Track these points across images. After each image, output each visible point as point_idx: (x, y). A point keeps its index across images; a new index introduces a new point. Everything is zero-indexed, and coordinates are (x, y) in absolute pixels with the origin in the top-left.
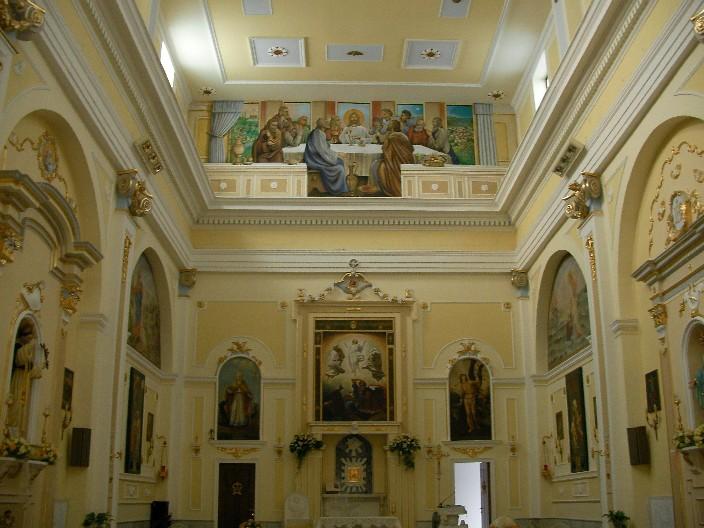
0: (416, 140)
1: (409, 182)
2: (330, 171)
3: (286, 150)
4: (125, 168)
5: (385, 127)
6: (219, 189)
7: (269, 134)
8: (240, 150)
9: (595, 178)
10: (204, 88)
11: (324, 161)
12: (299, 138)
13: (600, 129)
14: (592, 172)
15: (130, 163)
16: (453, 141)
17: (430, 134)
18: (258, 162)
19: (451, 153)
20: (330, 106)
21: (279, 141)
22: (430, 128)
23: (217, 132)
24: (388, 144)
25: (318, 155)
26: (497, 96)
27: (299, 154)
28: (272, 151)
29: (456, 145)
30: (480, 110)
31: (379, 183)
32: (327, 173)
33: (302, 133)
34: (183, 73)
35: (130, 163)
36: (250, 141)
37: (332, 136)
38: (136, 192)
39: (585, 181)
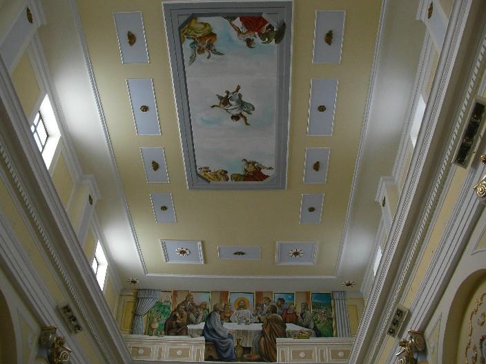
0: (288, 320)
1: (283, 352)
2: (222, 343)
3: (189, 327)
4: (48, 325)
5: (265, 310)
6: (138, 355)
7: (178, 315)
8: (156, 325)
9: (420, 334)
10: (131, 279)
11: (219, 336)
12: (200, 317)
13: (421, 296)
14: (416, 330)
15: (53, 320)
16: (316, 320)
17: (299, 315)
18: (168, 335)
19: (315, 328)
20: (224, 294)
21: (185, 319)
22: (299, 310)
23: (140, 312)
24: (268, 323)
25: (214, 331)
26: (349, 285)
27: (199, 330)
28: (179, 327)
29: (319, 322)
30: (336, 296)
31: (260, 352)
32: (220, 344)
33: (202, 314)
34: (115, 269)
35: (53, 320)
36: (164, 319)
37: (225, 317)
38: (54, 344)
39: (411, 338)
